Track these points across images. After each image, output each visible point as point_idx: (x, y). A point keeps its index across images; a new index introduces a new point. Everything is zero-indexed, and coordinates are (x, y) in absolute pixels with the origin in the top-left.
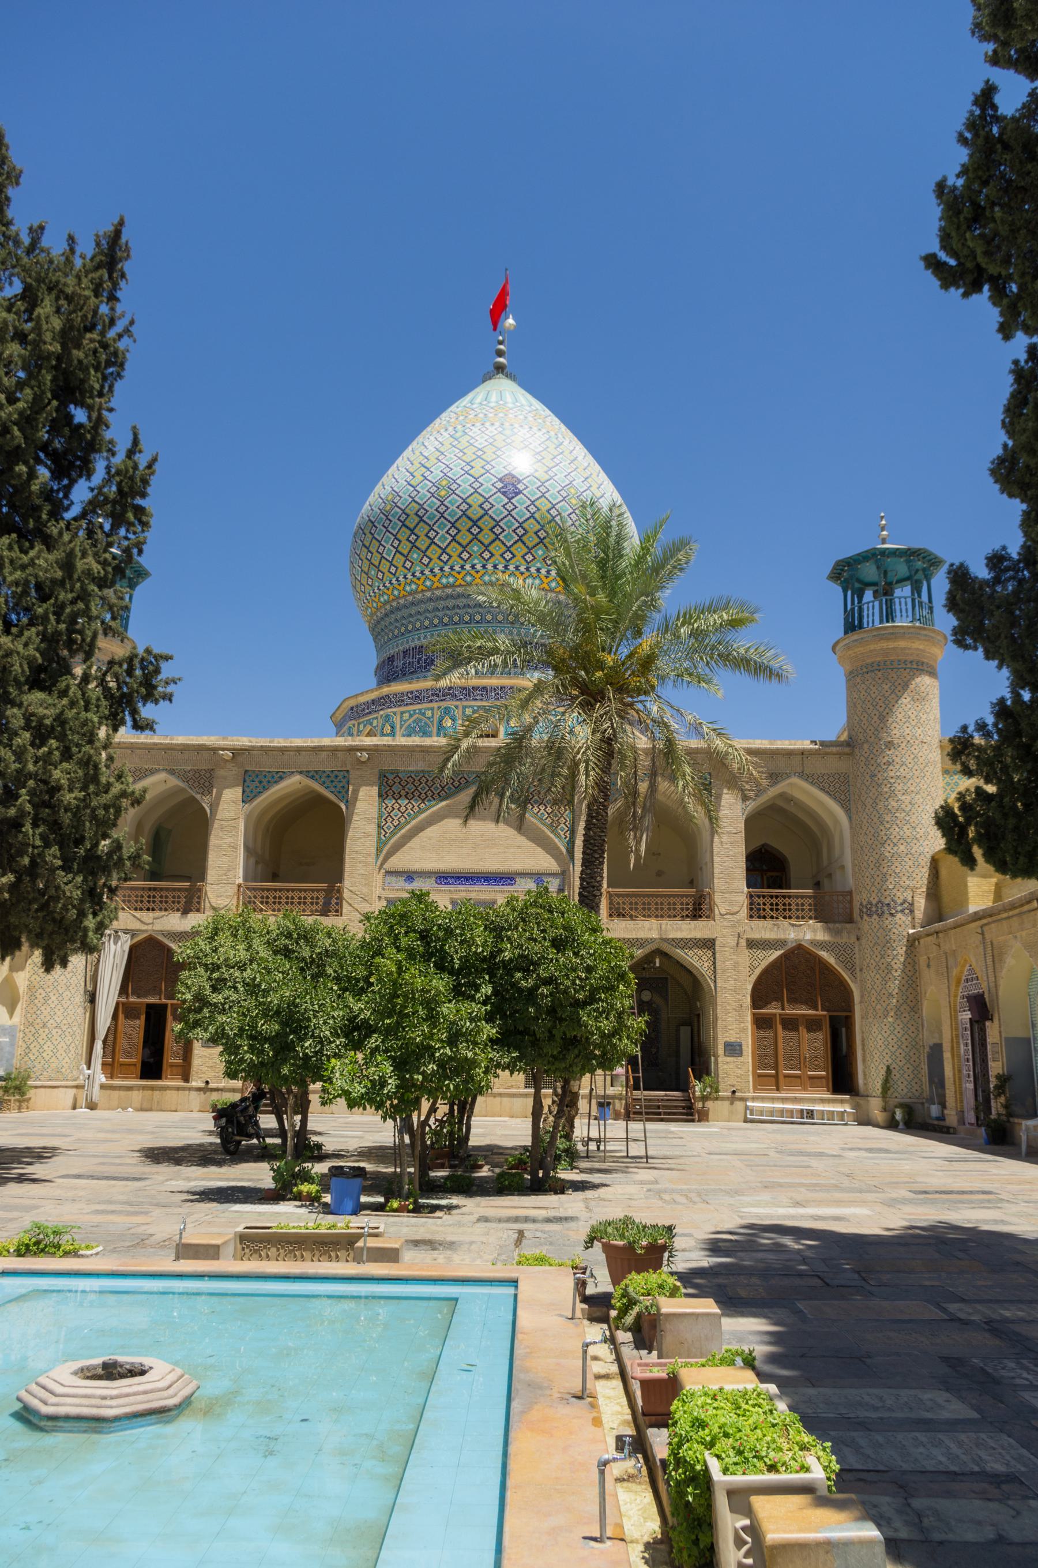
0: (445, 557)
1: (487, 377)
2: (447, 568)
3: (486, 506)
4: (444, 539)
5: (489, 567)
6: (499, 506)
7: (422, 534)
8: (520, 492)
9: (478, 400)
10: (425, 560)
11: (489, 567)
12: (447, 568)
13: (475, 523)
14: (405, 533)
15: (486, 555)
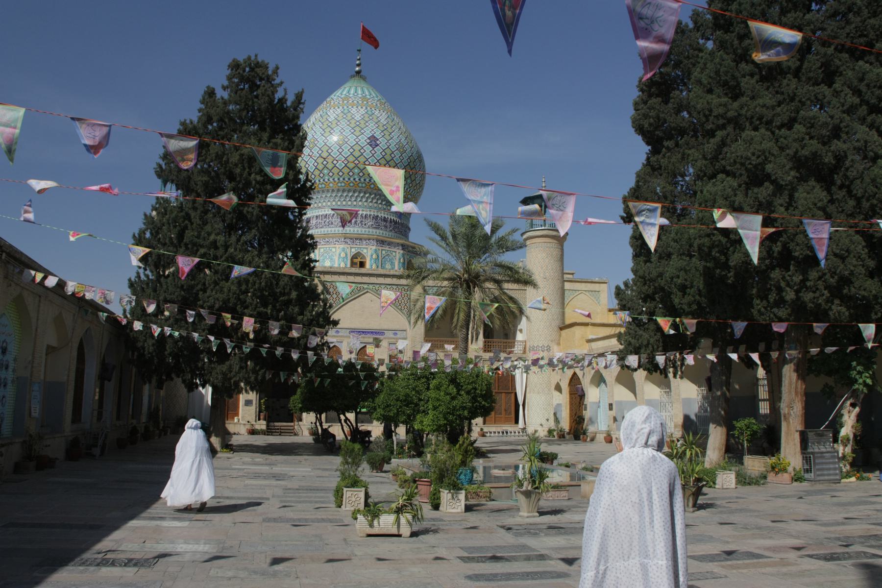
0: (341, 174)
1: (352, 76)
2: (341, 179)
3: (362, 151)
4: (340, 165)
5: (362, 180)
6: (368, 151)
7: (330, 161)
8: (378, 145)
9: (352, 92)
10: (331, 174)
11: (362, 180)
12: (341, 179)
13: (357, 159)
14: (320, 160)
15: (361, 174)
